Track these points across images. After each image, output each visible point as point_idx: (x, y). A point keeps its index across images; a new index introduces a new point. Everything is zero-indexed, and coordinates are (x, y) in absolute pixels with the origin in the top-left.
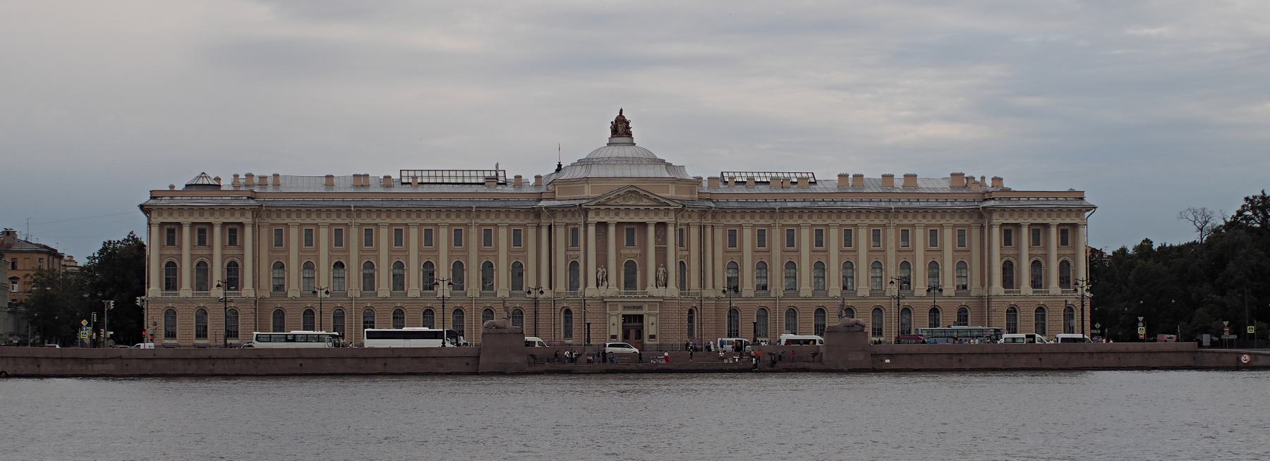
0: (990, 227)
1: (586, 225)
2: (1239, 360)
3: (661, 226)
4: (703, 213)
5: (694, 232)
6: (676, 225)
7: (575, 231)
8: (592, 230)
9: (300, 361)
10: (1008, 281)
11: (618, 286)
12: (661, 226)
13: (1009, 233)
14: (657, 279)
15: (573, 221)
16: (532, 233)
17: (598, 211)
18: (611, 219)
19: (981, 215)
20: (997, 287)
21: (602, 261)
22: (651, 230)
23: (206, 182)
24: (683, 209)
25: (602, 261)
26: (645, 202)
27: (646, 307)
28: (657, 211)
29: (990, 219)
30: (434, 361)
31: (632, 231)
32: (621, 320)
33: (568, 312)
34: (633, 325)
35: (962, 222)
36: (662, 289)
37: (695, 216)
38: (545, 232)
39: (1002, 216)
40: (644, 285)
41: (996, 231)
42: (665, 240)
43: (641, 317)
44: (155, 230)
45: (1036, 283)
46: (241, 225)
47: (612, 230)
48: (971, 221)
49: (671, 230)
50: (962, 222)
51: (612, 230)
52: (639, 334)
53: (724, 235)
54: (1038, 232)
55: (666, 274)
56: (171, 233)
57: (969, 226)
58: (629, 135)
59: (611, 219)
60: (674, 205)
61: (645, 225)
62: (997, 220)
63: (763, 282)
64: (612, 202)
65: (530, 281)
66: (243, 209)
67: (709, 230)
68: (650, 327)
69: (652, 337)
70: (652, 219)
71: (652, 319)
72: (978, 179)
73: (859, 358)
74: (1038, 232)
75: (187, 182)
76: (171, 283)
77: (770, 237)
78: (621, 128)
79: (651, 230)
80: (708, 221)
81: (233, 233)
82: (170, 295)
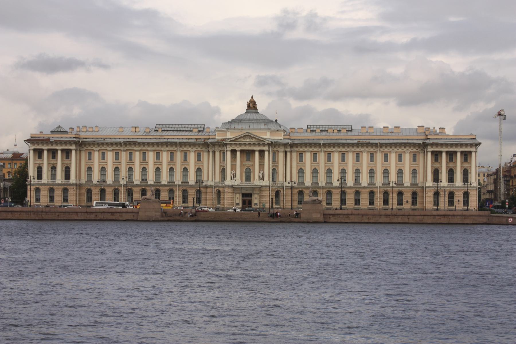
0: (427, 152)
1: (227, 151)
2: (507, 220)
3: (262, 152)
4: (285, 145)
5: (281, 155)
6: (269, 151)
7: (224, 153)
8: (229, 153)
9: (57, 214)
10: (436, 178)
11: (241, 180)
12: (262, 152)
13: (436, 155)
14: (259, 177)
15: (223, 149)
16: (206, 154)
17: (231, 145)
18: (238, 148)
19: (424, 146)
20: (430, 183)
21: (233, 167)
22: (257, 154)
23: (59, 130)
24: (272, 144)
25: (233, 167)
26: (254, 140)
28: (259, 145)
29: (427, 149)
30: (118, 214)
31: (248, 154)
33: (219, 192)
34: (247, 199)
35: (415, 150)
36: (261, 181)
37: (289, 147)
38: (211, 154)
40: (254, 180)
41: (429, 155)
44: (32, 152)
45: (451, 180)
46: (71, 150)
47: (238, 154)
48: (419, 150)
49: (266, 154)
50: (415, 150)
51: (238, 154)
52: (250, 202)
53: (297, 156)
54: (451, 155)
55: (263, 174)
56: (39, 153)
57: (418, 152)
58: (256, 109)
59: (238, 148)
61: (253, 151)
62: (430, 149)
63: (116, 176)
64: (239, 140)
65: (204, 178)
66: (70, 143)
67: (288, 154)
68: (255, 200)
69: (256, 204)
70: (257, 148)
71: (256, 196)
72: (432, 128)
73: (317, 216)
74: (451, 155)
75: (52, 130)
76: (40, 176)
77: (121, 156)
78: (252, 106)
79: (257, 154)
80: (288, 149)
81: (67, 153)
82: (66, 182)
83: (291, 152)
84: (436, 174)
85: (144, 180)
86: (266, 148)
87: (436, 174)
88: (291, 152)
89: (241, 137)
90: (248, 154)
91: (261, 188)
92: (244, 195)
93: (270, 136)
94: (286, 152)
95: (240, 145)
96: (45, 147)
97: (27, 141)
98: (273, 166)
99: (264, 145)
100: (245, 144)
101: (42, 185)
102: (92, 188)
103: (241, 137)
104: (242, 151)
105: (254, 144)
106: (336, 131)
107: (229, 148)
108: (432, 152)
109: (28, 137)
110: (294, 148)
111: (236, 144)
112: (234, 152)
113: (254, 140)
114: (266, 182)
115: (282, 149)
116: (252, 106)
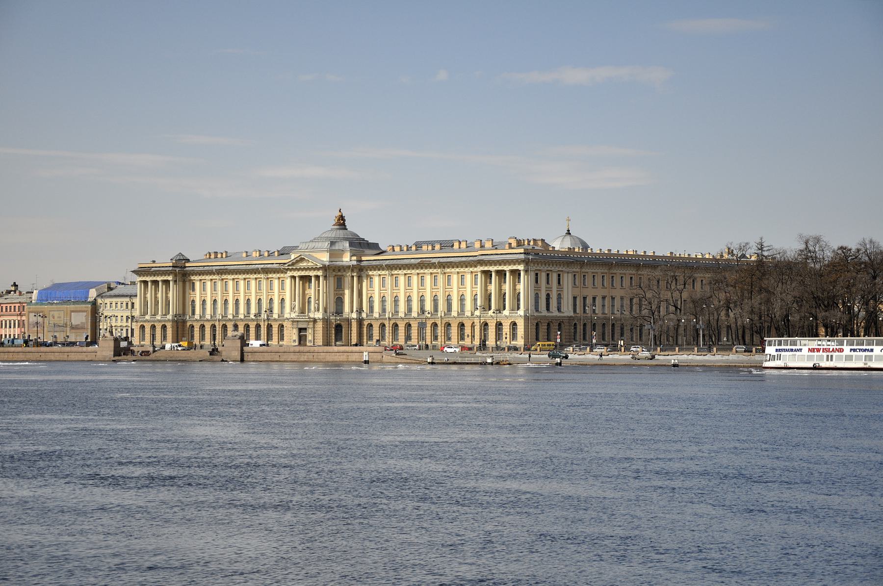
17: (291, 270)
18: (296, 274)
31: (306, 279)
39: (481, 265)
49: (321, 278)
58: (344, 224)
60: (319, 265)
69: (310, 341)
78: (341, 222)
85: (423, 311)
86: (320, 273)
89: (297, 262)
91: (315, 321)
92: (300, 330)
95: (298, 270)
96: (148, 279)
98: (335, 295)
99: (318, 269)
100: (303, 269)
101: (145, 321)
102: (194, 324)
103: (297, 262)
104: (301, 277)
106: (430, 248)
107: (290, 274)
109: (136, 268)
116: (341, 222)
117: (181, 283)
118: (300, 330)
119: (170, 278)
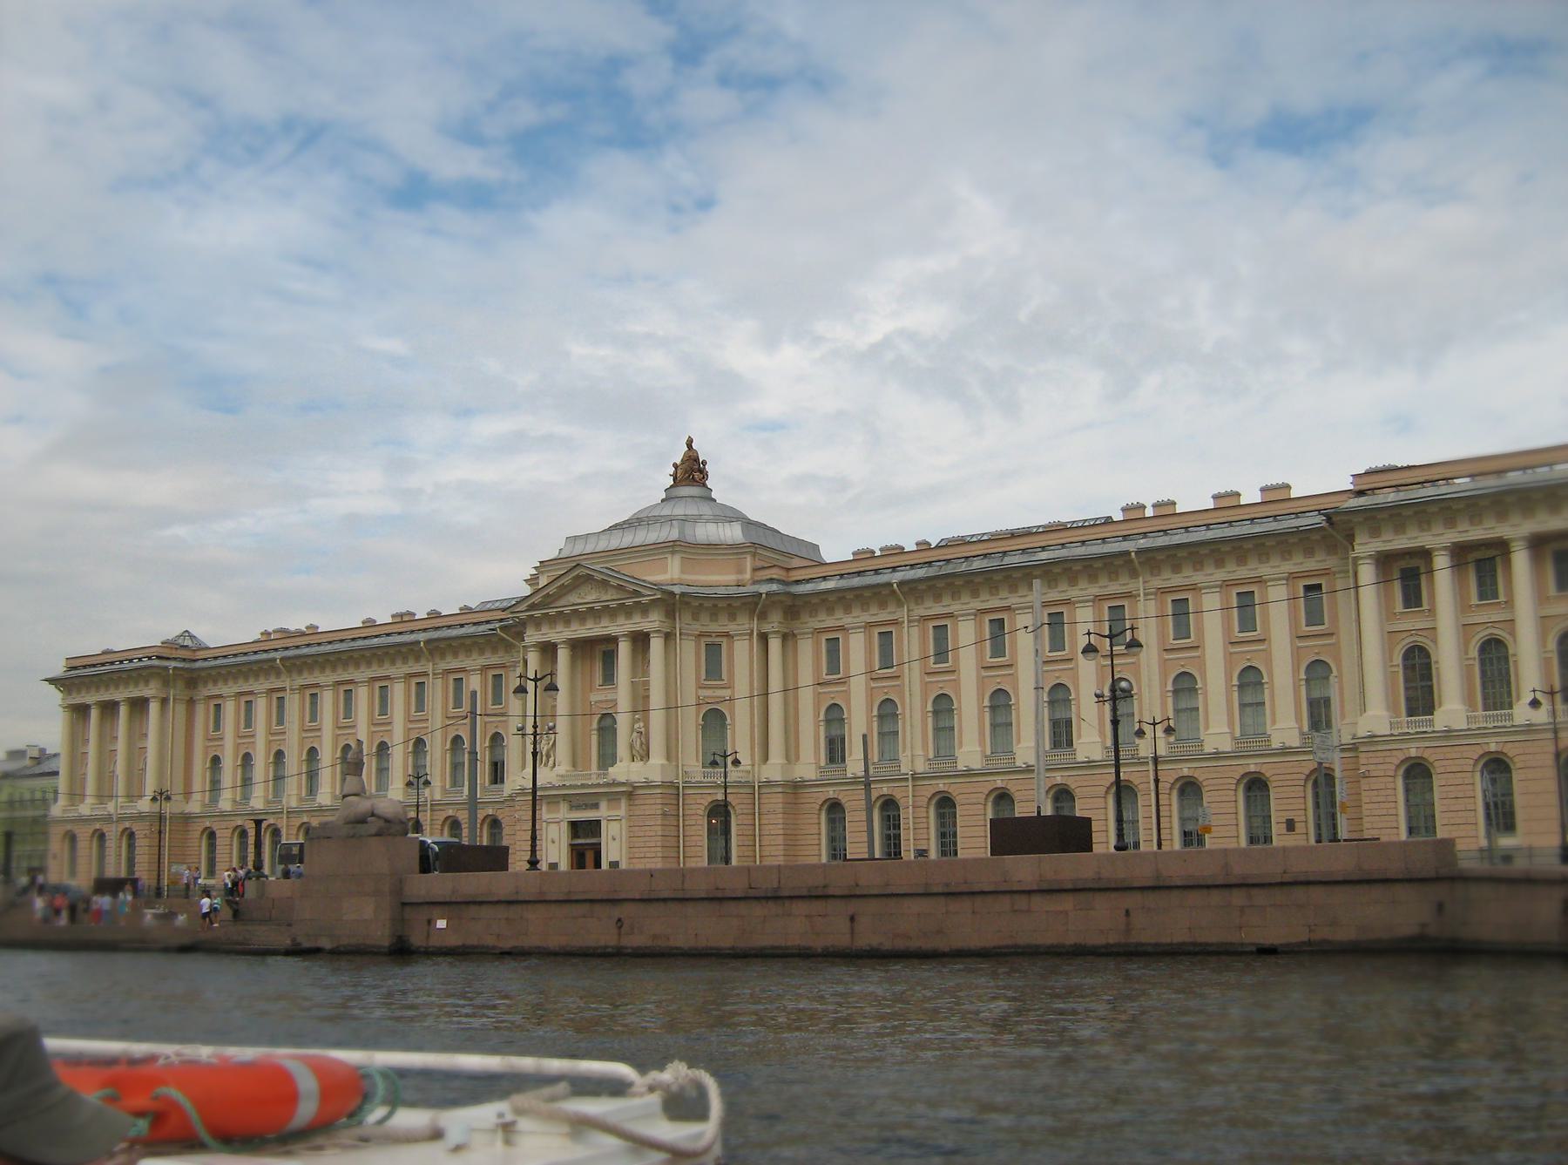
3: (641, 641)
4: (753, 605)
13: (1407, 574)
17: (538, 623)
22: (624, 649)
27: (603, 805)
28: (627, 611)
31: (596, 652)
32: (565, 826)
35: (1311, 564)
39: (1375, 532)
41: (1367, 573)
42: (646, 673)
43: (598, 822)
47: (563, 655)
49: (656, 644)
50: (1311, 564)
51: (563, 655)
62: (1366, 546)
67: (775, 644)
70: (619, 627)
78: (691, 471)
79: (624, 649)
80: (774, 623)
83: (788, 638)
84: (1417, 675)
86: (652, 622)
87: (1417, 675)
88: (788, 638)
89: (565, 590)
90: (596, 652)
93: (683, 572)
94: (764, 638)
95: (565, 618)
97: (51, 681)
99: (644, 609)
100: (580, 616)
105: (610, 612)
108: (1384, 561)
109: (59, 670)
110: (805, 617)
111: (551, 620)
112: (548, 650)
113: (608, 596)
114: (654, 769)
115: (743, 624)
116: (691, 471)
117: (181, 709)
118: (576, 828)
119: (150, 690)
